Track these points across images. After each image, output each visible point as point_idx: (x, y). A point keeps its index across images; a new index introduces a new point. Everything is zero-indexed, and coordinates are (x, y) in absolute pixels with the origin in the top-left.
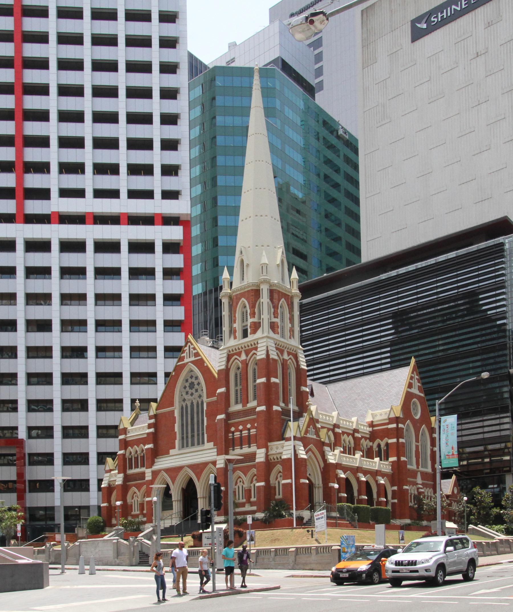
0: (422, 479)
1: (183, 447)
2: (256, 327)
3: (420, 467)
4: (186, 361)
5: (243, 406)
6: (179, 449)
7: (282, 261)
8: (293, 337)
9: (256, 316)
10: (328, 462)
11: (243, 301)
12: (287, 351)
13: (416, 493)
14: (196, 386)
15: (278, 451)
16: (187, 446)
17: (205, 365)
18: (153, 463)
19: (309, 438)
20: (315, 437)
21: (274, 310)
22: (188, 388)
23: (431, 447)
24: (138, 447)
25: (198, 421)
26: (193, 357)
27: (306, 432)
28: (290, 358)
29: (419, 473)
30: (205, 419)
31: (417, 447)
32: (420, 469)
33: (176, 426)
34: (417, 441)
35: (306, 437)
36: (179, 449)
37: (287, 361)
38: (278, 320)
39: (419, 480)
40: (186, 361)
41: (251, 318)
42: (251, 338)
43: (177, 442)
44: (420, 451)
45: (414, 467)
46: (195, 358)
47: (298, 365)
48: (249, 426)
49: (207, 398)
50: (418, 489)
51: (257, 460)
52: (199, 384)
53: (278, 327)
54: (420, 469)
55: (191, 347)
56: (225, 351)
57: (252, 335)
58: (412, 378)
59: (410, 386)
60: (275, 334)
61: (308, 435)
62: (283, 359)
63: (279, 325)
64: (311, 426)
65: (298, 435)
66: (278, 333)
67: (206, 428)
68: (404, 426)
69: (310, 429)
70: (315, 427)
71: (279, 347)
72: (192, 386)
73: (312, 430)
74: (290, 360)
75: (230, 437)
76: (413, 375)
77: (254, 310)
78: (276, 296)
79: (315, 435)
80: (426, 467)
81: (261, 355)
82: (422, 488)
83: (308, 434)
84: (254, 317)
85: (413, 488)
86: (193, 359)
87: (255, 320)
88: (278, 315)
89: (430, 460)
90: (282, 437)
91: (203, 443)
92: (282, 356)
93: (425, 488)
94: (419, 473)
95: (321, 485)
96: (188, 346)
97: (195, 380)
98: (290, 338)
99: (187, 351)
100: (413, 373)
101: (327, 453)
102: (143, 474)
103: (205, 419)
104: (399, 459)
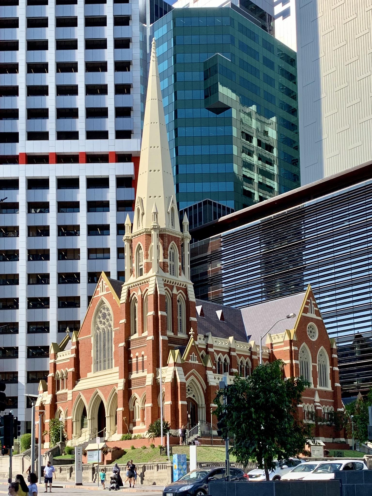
0: (320, 397)
1: (97, 370)
2: (148, 266)
3: (318, 386)
4: (100, 294)
5: (139, 335)
6: (94, 372)
7: (172, 209)
8: (184, 274)
9: (149, 257)
10: (209, 385)
11: (139, 245)
12: (176, 287)
13: (314, 410)
14: (108, 317)
15: (163, 376)
16: (100, 370)
17: (114, 298)
18: (74, 385)
19: (191, 363)
20: (197, 362)
21: (164, 252)
22: (101, 319)
23: (331, 367)
24: (64, 370)
25: (108, 348)
26: (105, 291)
27: (188, 358)
28: (180, 293)
29: (317, 392)
30: (113, 346)
31: (314, 367)
33: (92, 351)
34: (314, 361)
35: (189, 363)
36: (94, 372)
37: (176, 295)
38: (168, 260)
39: (317, 398)
40: (100, 294)
41: (145, 259)
42: (145, 276)
43: (92, 365)
44: (318, 370)
46: (106, 292)
47: (188, 298)
48: (143, 353)
49: (114, 328)
50: (315, 406)
51: (146, 384)
52: (109, 315)
53: (168, 266)
54: (318, 387)
55: (104, 282)
56: (126, 287)
57: (145, 274)
58: (307, 303)
59: (306, 310)
60: (165, 272)
61: (190, 361)
62: (173, 294)
63: (169, 264)
64: (193, 353)
65: (179, 361)
66: (168, 272)
67: (114, 354)
68: (299, 349)
69: (192, 356)
70: (197, 354)
71: (169, 283)
72: (104, 316)
73: (195, 356)
74: (180, 294)
75: (129, 363)
76: (309, 301)
77: (148, 252)
78: (166, 240)
80: (326, 386)
81: (151, 291)
82: (319, 406)
84: (147, 258)
85: (310, 406)
86: (105, 293)
87: (149, 261)
88: (168, 256)
89: (330, 379)
90: (165, 364)
91: (112, 368)
92: (172, 291)
93: (324, 406)
94: (317, 392)
95: (204, 405)
96: (101, 281)
97: (107, 311)
98: (180, 275)
99: (101, 286)
100: (308, 298)
101: (209, 376)
102: (66, 393)
103: (113, 346)
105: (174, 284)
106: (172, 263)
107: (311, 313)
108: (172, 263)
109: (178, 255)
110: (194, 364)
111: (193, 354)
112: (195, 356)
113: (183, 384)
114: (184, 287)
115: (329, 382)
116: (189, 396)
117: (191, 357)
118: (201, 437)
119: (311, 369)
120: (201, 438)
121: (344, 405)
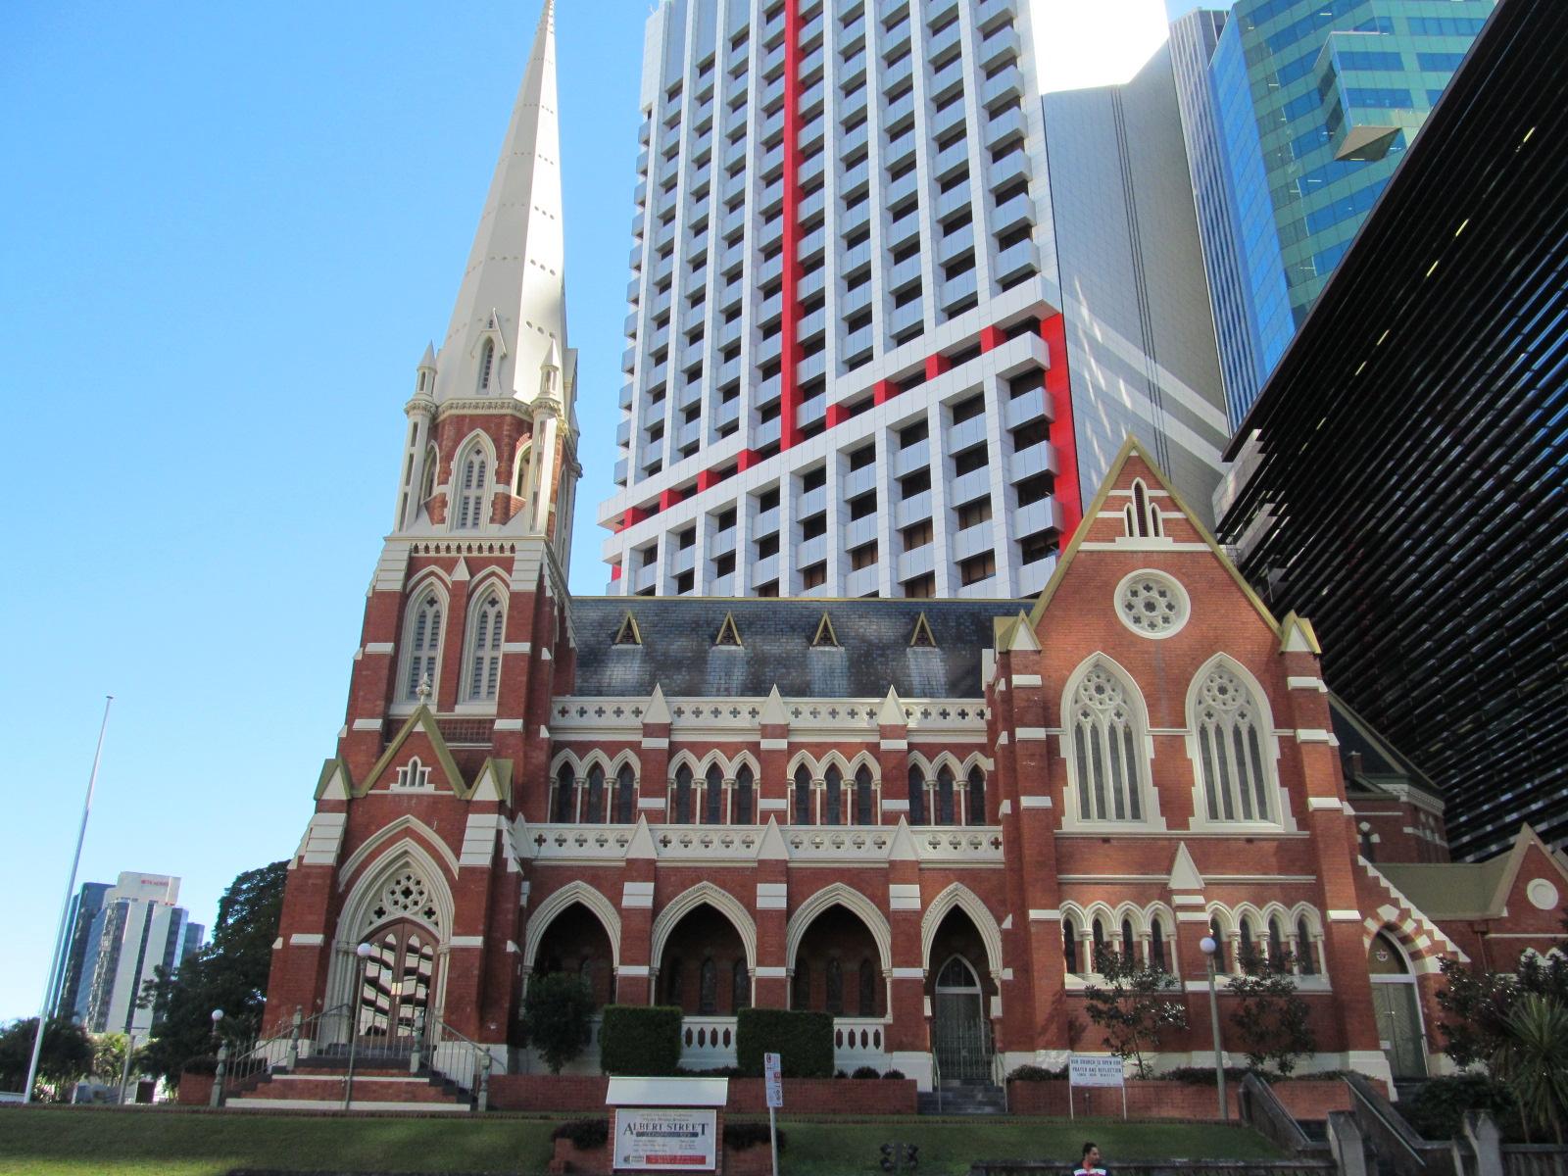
12: (466, 560)
19: (398, 795)
20: (429, 789)
23: (1288, 732)
28: (493, 574)
32: (1200, 823)
45: (1154, 823)
53: (444, 504)
54: (1200, 823)
61: (395, 788)
62: (454, 583)
64: (416, 758)
66: (442, 521)
69: (409, 768)
79: (430, 782)
83: (392, 785)
89: (1283, 784)
104: (1016, 804)
105: (465, 553)
106: (473, 493)
107: (1131, 534)
108: (473, 493)
109: (492, 465)
110: (410, 797)
111: (415, 764)
112: (420, 768)
113: (320, 870)
114: (508, 554)
115: (1279, 796)
116: (399, 913)
117: (405, 774)
118: (291, 1068)
119: (1147, 750)
120: (293, 1072)
121: (1395, 893)
